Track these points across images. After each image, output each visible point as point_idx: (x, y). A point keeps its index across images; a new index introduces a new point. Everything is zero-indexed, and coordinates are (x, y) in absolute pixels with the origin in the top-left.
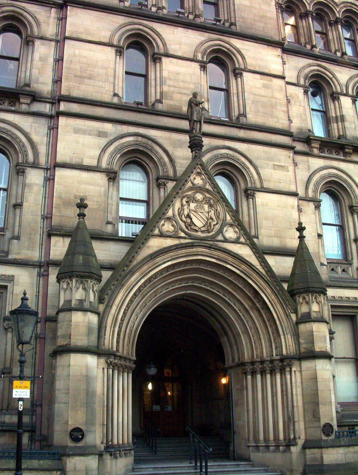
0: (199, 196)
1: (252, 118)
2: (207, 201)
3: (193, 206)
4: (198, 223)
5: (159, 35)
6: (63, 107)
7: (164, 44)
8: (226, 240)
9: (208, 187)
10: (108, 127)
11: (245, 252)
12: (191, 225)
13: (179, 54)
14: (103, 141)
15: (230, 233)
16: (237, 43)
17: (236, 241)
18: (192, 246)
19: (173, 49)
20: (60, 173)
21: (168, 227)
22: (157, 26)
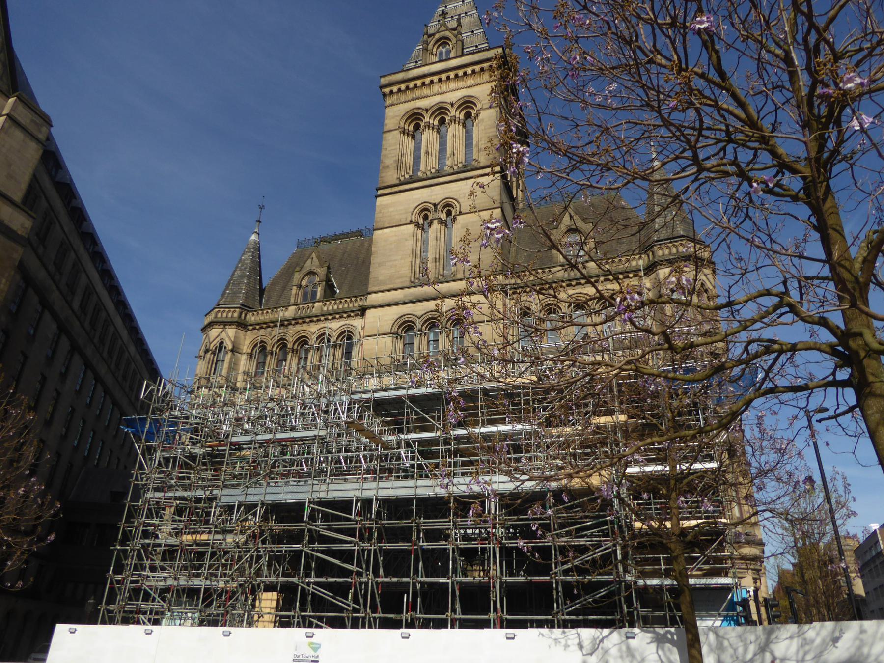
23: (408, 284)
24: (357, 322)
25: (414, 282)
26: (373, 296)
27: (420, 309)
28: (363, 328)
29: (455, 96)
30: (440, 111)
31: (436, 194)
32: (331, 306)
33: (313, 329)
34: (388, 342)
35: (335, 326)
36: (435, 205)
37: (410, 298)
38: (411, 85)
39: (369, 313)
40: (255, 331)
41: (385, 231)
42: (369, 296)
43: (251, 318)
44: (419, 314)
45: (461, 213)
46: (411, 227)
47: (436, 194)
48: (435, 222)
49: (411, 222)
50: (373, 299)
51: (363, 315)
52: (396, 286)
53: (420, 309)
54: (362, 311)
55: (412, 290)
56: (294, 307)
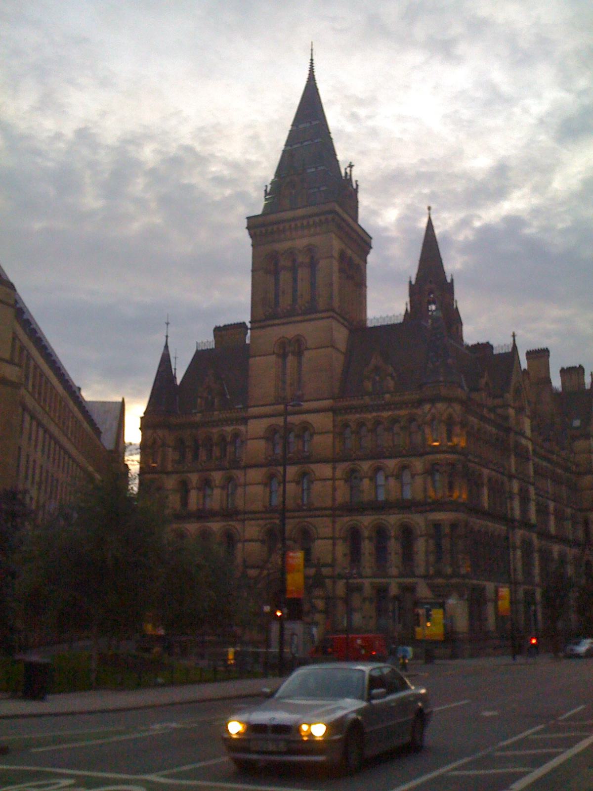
1: (317, 504)
6: (246, 516)
10: (261, 522)
16: (312, 466)
20: (246, 544)
24: (242, 428)
26: (252, 409)
29: (301, 243)
30: (291, 253)
31: (290, 331)
34: (262, 444)
36: (290, 341)
38: (270, 229)
39: (250, 422)
41: (257, 358)
42: (249, 409)
45: (307, 349)
46: (274, 357)
47: (290, 331)
48: (290, 354)
49: (274, 353)
51: (246, 423)
54: (245, 420)
55: (276, 407)
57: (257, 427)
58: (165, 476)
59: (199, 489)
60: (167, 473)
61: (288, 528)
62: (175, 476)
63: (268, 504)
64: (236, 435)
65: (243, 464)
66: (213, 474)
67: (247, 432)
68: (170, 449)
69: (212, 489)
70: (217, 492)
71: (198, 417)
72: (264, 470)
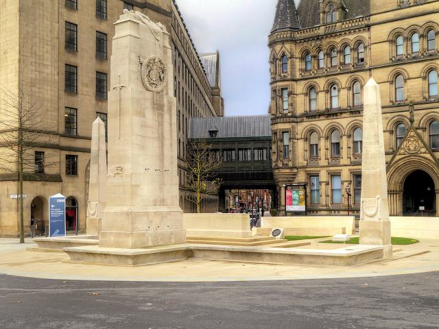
0: (412, 139)
2: (415, 140)
3: (410, 143)
4: (412, 148)
5: (405, 71)
7: (408, 74)
8: (421, 153)
9: (415, 135)
10: (388, 115)
11: (428, 156)
12: (409, 150)
13: (414, 76)
14: (388, 120)
15: (423, 150)
17: (425, 153)
18: (408, 156)
19: (412, 75)
21: (402, 151)
22: (404, 67)
23: (396, 7)
24: (365, 35)
25: (400, 6)
26: (374, 16)
27: (405, 24)
28: (370, 38)
32: (347, 25)
33: (338, 40)
34: (386, 45)
35: (351, 37)
37: (398, 17)
39: (372, 28)
40: (301, 44)
42: (371, 17)
43: (298, 35)
44: (405, 27)
50: (374, 19)
52: (388, 9)
53: (405, 24)
54: (368, 27)
55: (399, 11)
56: (323, 27)
57: (380, 32)
58: (294, 83)
59: (327, 92)
60: (296, 80)
61: (416, 118)
62: (303, 83)
63: (394, 100)
64: (359, 42)
65: (367, 67)
66: (339, 77)
67: (370, 38)
68: (298, 60)
69: (339, 91)
70: (344, 92)
71: (321, 31)
72: (391, 69)
